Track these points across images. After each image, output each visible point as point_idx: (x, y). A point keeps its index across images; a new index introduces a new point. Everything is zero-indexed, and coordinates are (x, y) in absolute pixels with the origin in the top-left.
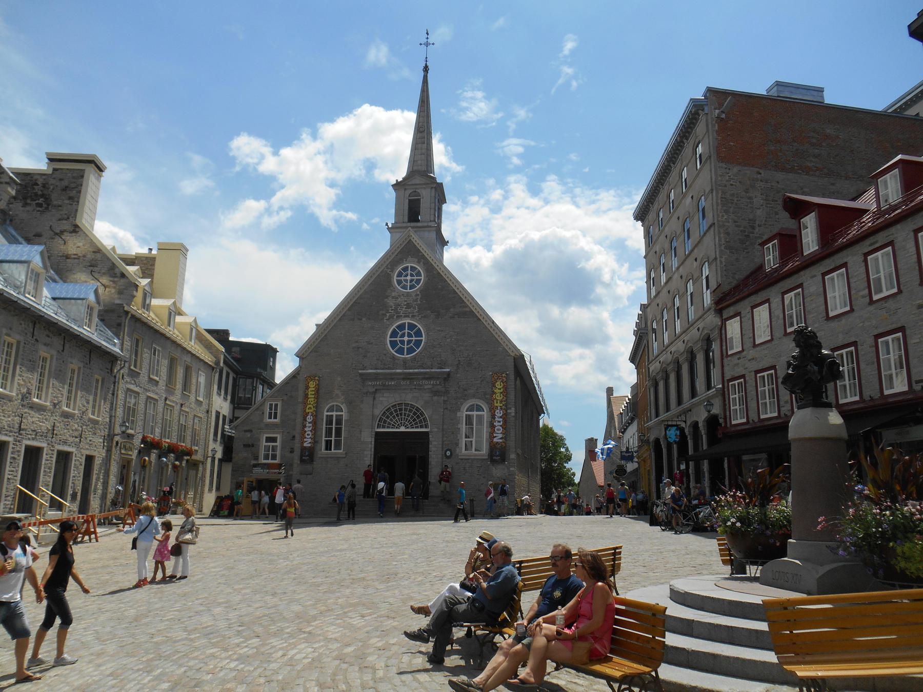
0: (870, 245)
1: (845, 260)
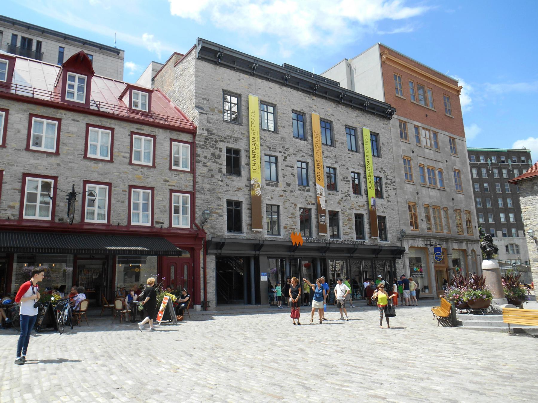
0: (136, 129)
1: (112, 126)
